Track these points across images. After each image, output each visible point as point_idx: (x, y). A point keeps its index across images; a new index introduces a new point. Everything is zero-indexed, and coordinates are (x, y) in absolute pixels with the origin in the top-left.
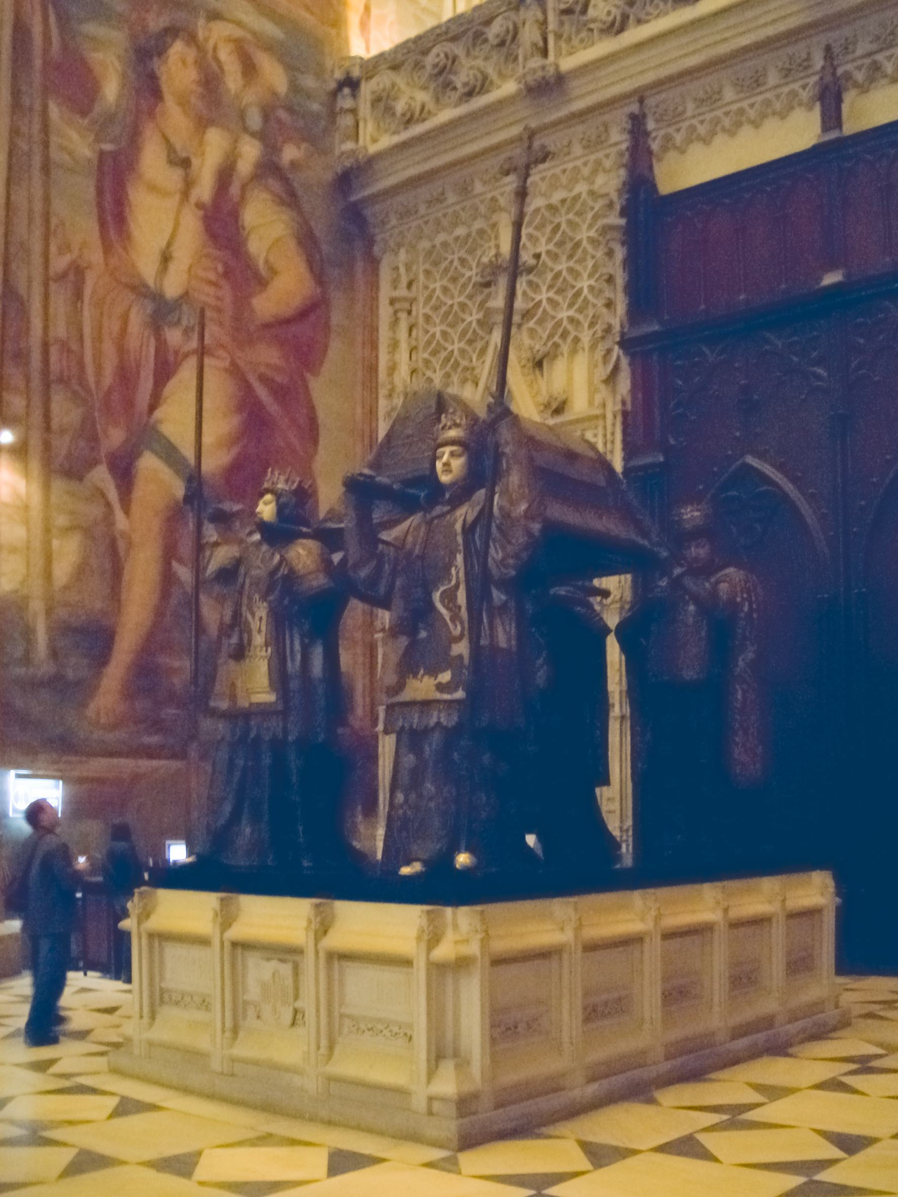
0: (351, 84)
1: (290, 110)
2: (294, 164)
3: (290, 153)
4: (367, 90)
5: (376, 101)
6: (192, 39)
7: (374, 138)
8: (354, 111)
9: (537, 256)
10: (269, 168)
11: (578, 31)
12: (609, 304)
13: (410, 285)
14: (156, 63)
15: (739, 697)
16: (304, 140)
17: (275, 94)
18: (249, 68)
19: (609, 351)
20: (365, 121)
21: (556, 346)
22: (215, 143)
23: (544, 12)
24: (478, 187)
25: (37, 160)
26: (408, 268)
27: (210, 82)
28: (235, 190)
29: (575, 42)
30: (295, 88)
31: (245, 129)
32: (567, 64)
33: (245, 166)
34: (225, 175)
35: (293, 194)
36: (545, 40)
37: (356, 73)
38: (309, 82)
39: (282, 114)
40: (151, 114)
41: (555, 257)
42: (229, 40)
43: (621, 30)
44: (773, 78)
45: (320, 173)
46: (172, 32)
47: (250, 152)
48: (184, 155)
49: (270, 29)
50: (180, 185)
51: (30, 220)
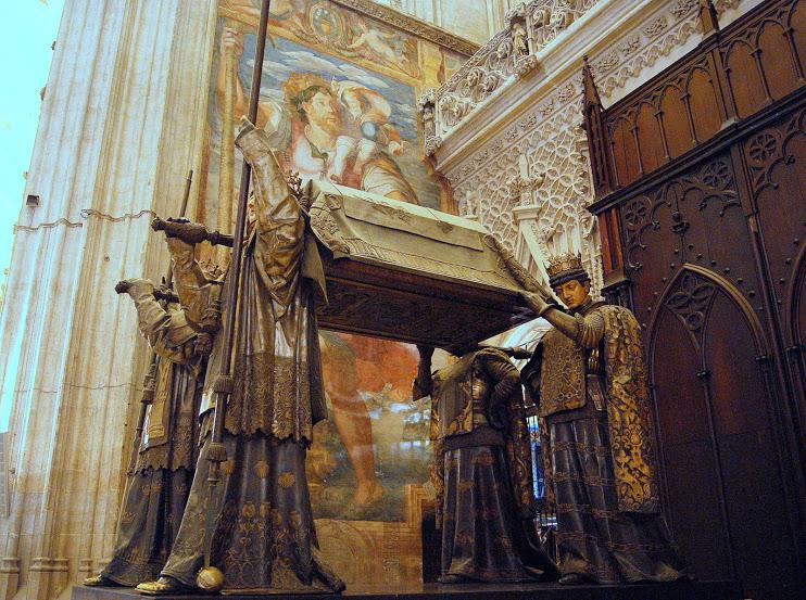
0: (430, 105)
1: (394, 124)
2: (395, 152)
3: (393, 147)
4: (438, 107)
5: (445, 109)
6: (328, 91)
7: (443, 130)
8: (431, 119)
9: (543, 175)
10: (380, 155)
11: (546, 36)
12: (586, 190)
13: (474, 211)
14: (304, 105)
15: (617, 418)
16: (403, 139)
17: (383, 117)
18: (365, 104)
19: (588, 219)
20: (439, 123)
21: (560, 226)
22: (344, 145)
23: (525, 30)
24: (506, 145)
25: (226, 159)
26: (472, 200)
27: (340, 113)
28: (357, 169)
29: (546, 41)
30: (396, 112)
31: (365, 136)
32: (540, 55)
33: (364, 155)
34: (350, 162)
35: (398, 169)
36: (527, 46)
37: (431, 98)
38: (405, 108)
39: (387, 126)
40: (302, 132)
41: (554, 173)
42: (351, 90)
43: (570, 23)
44: (671, 21)
45: (417, 156)
46: (315, 89)
47: (367, 148)
48: (323, 151)
49: (378, 83)
50: (321, 168)
51: (220, 191)
